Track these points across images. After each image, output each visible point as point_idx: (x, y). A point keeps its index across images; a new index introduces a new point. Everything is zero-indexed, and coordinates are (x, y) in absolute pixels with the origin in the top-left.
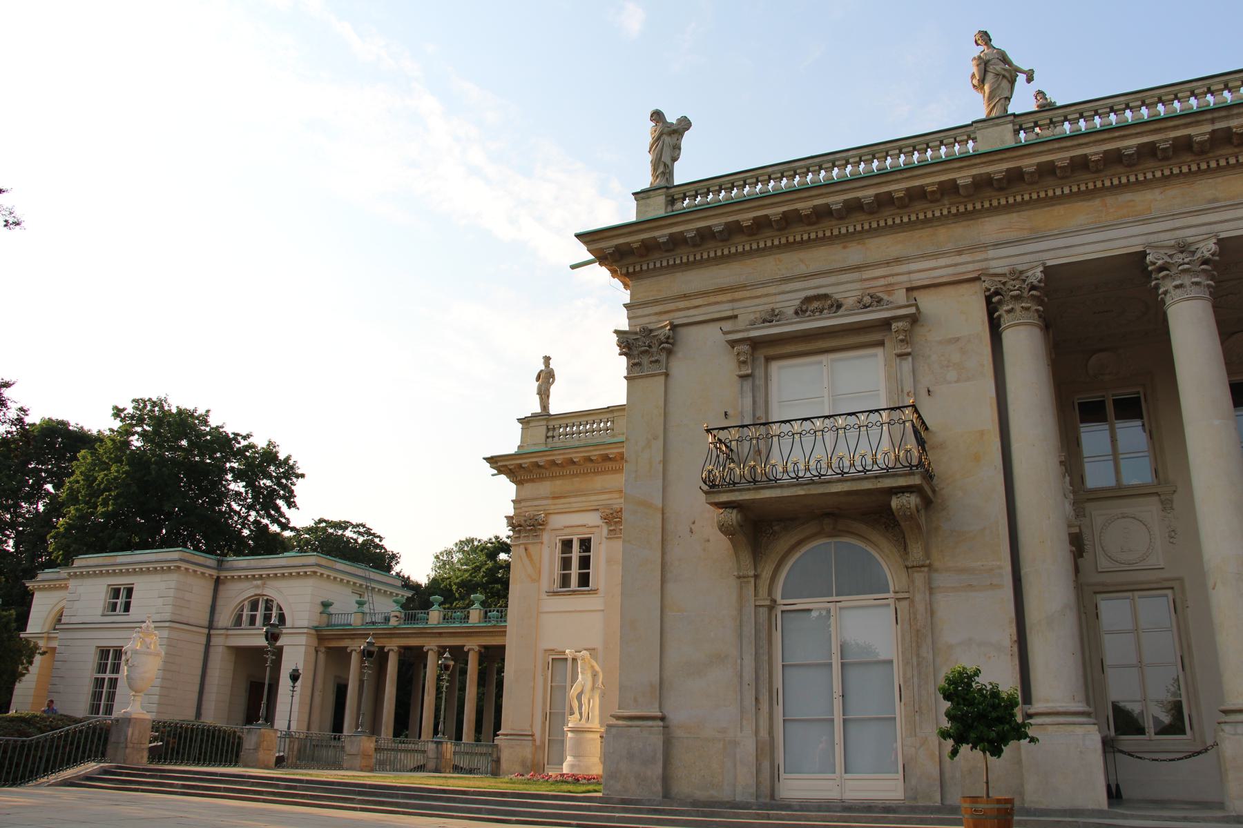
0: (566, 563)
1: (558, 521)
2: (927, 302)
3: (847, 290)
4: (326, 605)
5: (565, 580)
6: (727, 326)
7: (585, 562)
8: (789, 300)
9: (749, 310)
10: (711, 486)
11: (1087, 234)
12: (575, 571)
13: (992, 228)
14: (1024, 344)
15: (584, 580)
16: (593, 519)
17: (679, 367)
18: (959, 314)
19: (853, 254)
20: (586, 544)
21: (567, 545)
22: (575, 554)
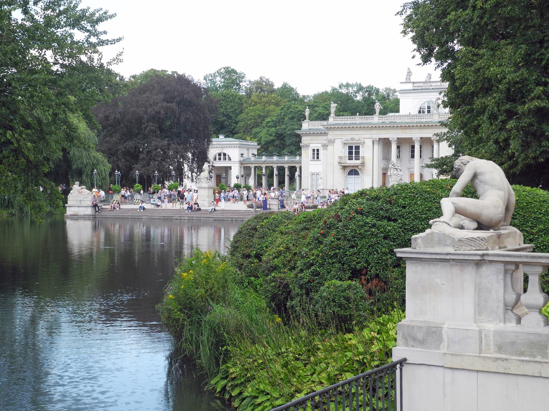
0: (314, 154)
1: (311, 145)
2: (365, 140)
3: (356, 138)
4: (242, 154)
5: (314, 158)
6: (341, 140)
7: (318, 154)
8: (349, 138)
9: (345, 138)
10: (340, 163)
11: (384, 134)
12: (316, 156)
13: (374, 132)
14: (376, 147)
15: (318, 158)
16: (320, 145)
17: (335, 144)
18: (369, 143)
19: (357, 132)
20: (318, 150)
21: (314, 150)
22: (316, 152)
